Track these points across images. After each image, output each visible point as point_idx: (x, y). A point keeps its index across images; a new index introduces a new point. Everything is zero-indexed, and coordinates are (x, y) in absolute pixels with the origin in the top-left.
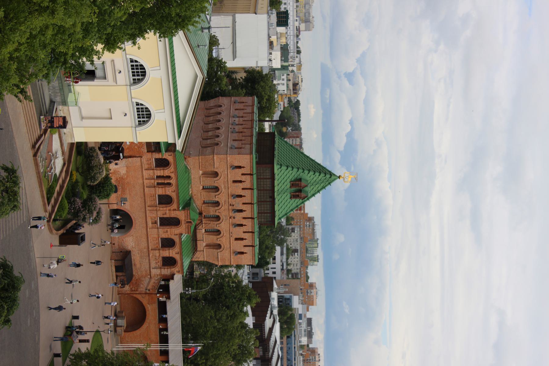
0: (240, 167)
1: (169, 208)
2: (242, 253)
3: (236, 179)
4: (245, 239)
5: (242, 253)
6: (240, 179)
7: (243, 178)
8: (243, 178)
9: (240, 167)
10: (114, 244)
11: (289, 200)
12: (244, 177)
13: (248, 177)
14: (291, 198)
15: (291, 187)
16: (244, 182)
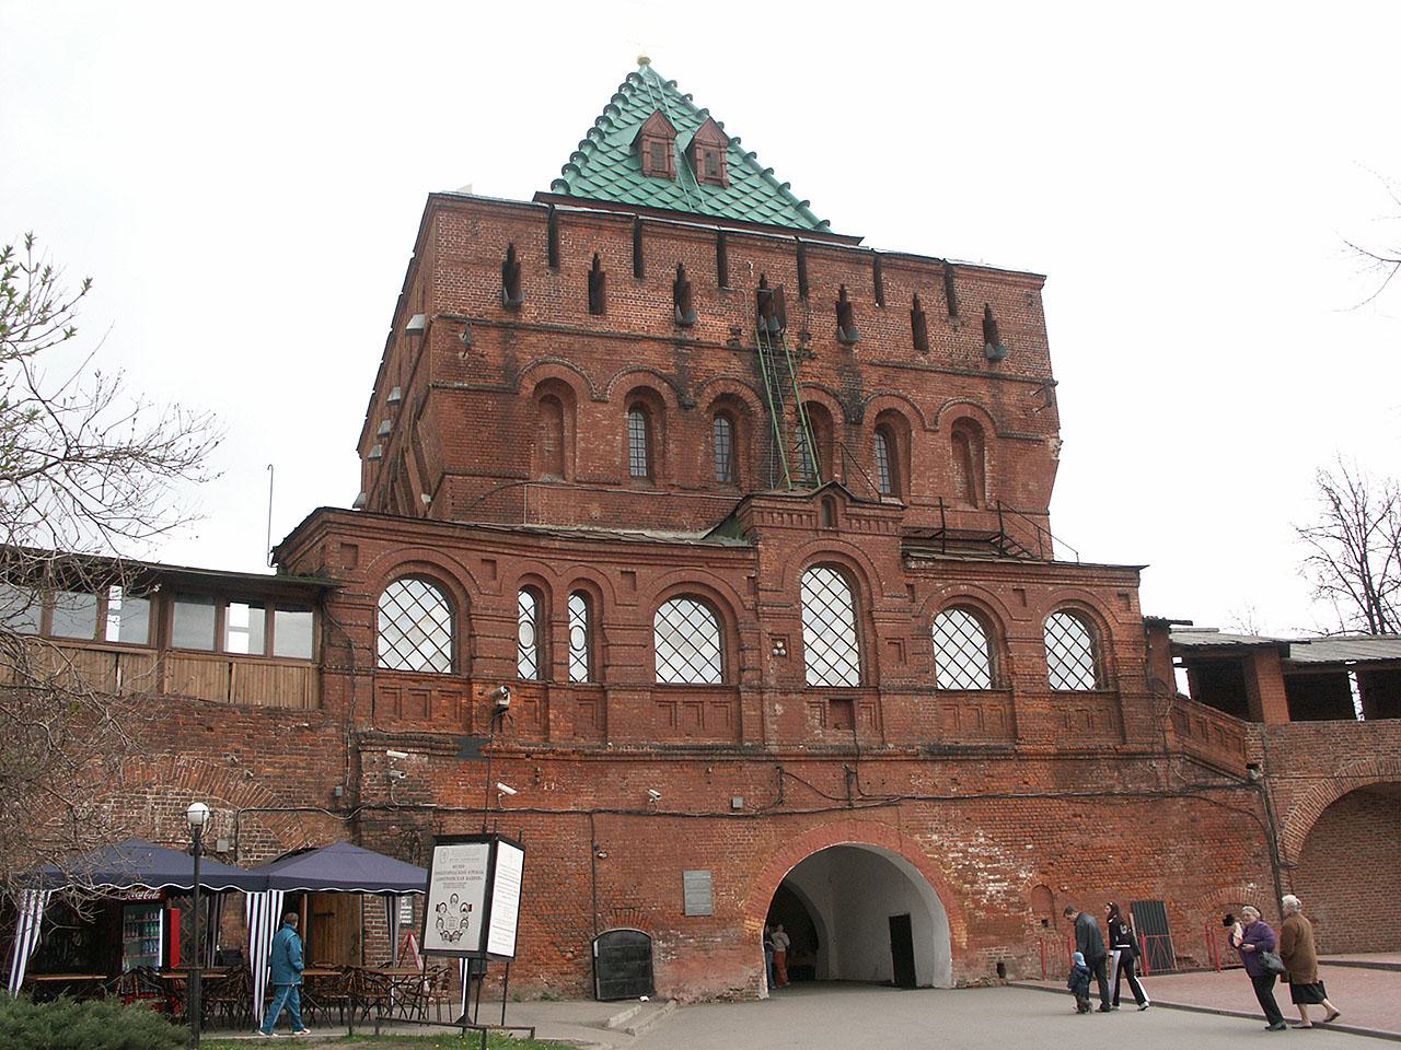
0: (511, 273)
1: (745, 617)
2: (989, 329)
3: (584, 304)
4: (916, 302)
5: (989, 329)
6: (583, 283)
7: (576, 263)
8: (576, 263)
9: (511, 273)
10: (1001, 968)
11: (731, 191)
12: (566, 261)
13: (566, 239)
14: (722, 185)
15: (670, 177)
16: (596, 262)
